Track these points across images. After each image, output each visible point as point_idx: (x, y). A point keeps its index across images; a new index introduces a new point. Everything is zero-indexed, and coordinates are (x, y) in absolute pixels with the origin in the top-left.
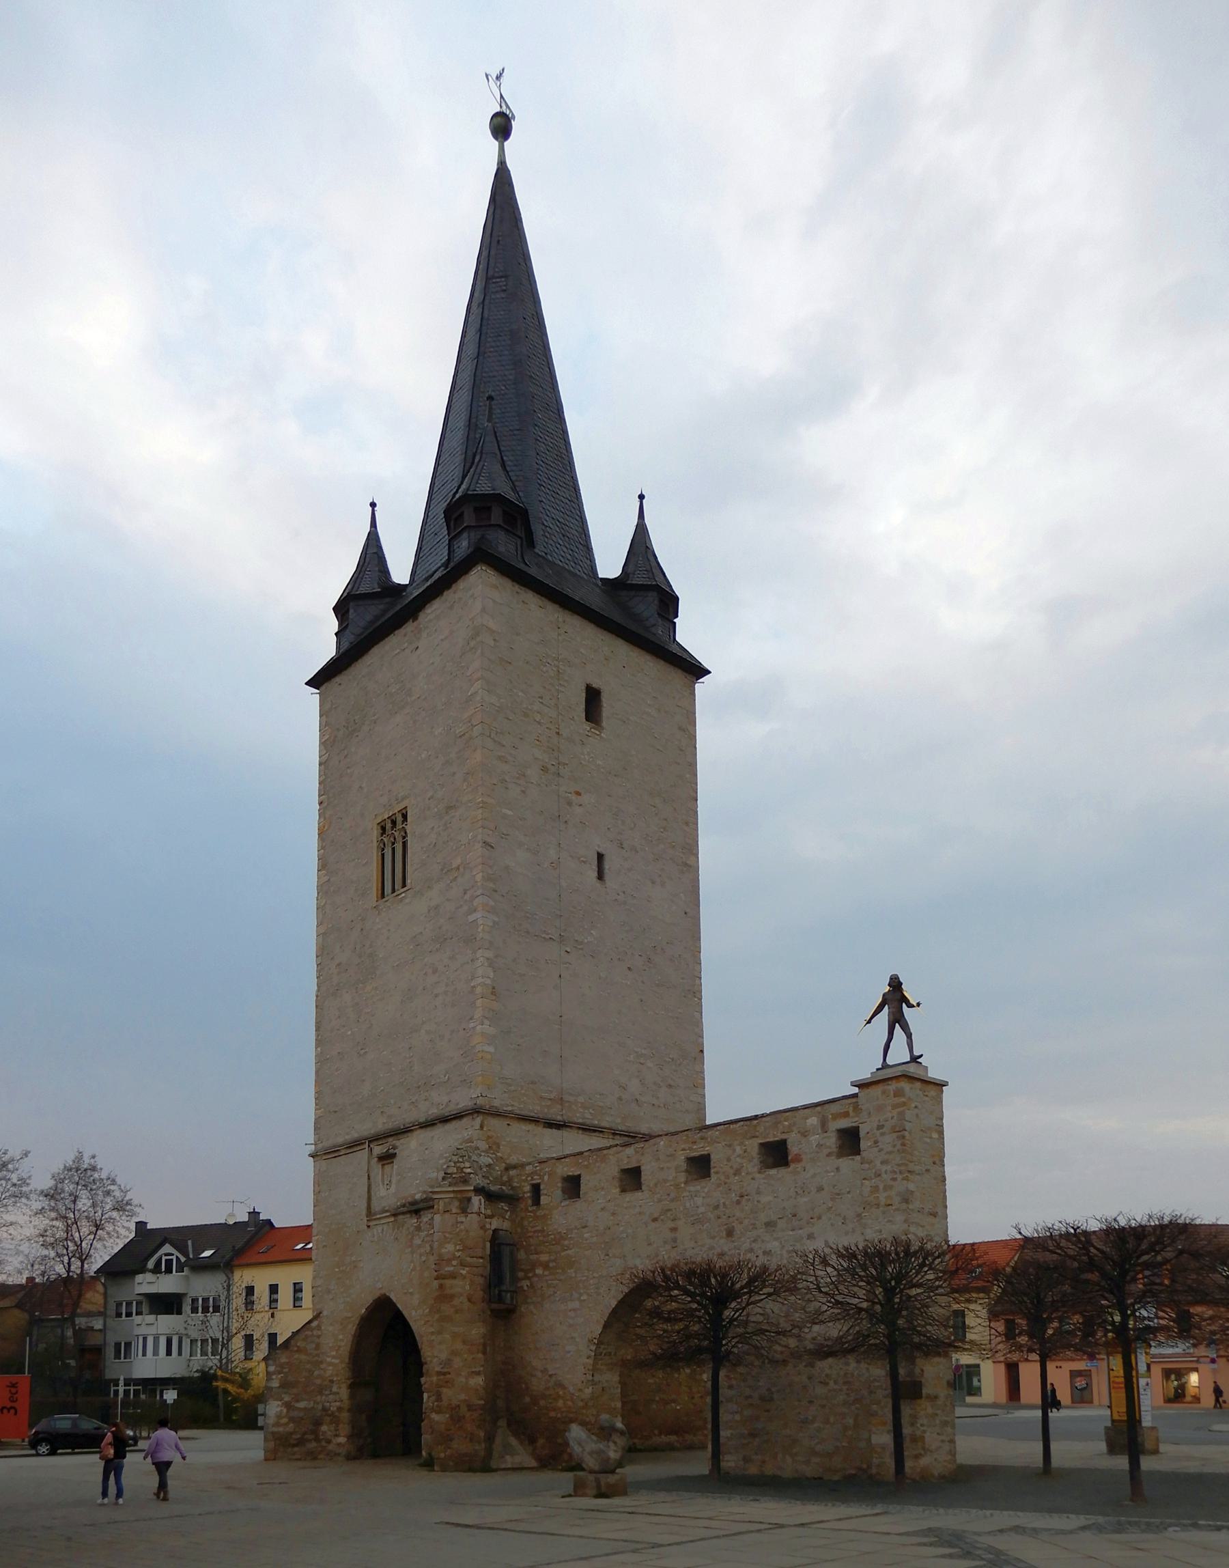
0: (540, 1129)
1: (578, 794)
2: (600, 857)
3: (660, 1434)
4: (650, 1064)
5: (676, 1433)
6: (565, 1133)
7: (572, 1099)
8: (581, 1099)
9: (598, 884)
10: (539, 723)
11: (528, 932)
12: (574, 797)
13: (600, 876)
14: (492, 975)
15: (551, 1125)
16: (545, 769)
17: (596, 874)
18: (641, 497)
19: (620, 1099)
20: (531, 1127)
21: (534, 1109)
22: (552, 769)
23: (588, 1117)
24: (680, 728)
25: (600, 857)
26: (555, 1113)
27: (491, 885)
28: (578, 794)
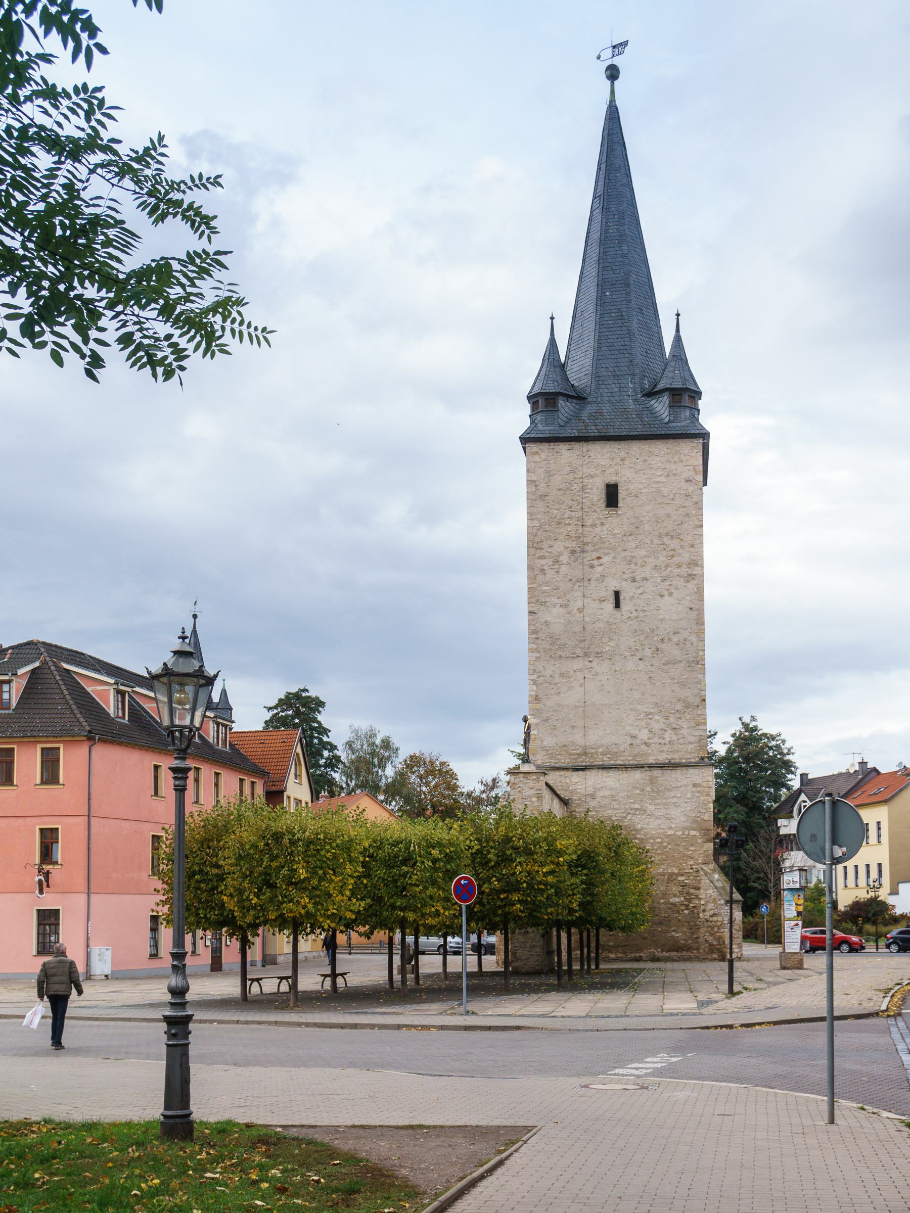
0: (570, 773)
1: (599, 558)
2: (617, 594)
3: (662, 951)
4: (657, 718)
5: (677, 951)
6: (588, 772)
7: (593, 751)
8: (601, 750)
9: (615, 612)
10: (569, 524)
11: (561, 657)
12: (596, 562)
13: (617, 605)
14: (535, 689)
15: (576, 769)
16: (573, 552)
17: (613, 605)
18: (678, 315)
19: (632, 744)
20: (562, 773)
21: (565, 761)
22: (578, 550)
23: (607, 761)
24: (687, 481)
25: (617, 594)
26: (581, 762)
27: (535, 636)
28: (599, 558)
